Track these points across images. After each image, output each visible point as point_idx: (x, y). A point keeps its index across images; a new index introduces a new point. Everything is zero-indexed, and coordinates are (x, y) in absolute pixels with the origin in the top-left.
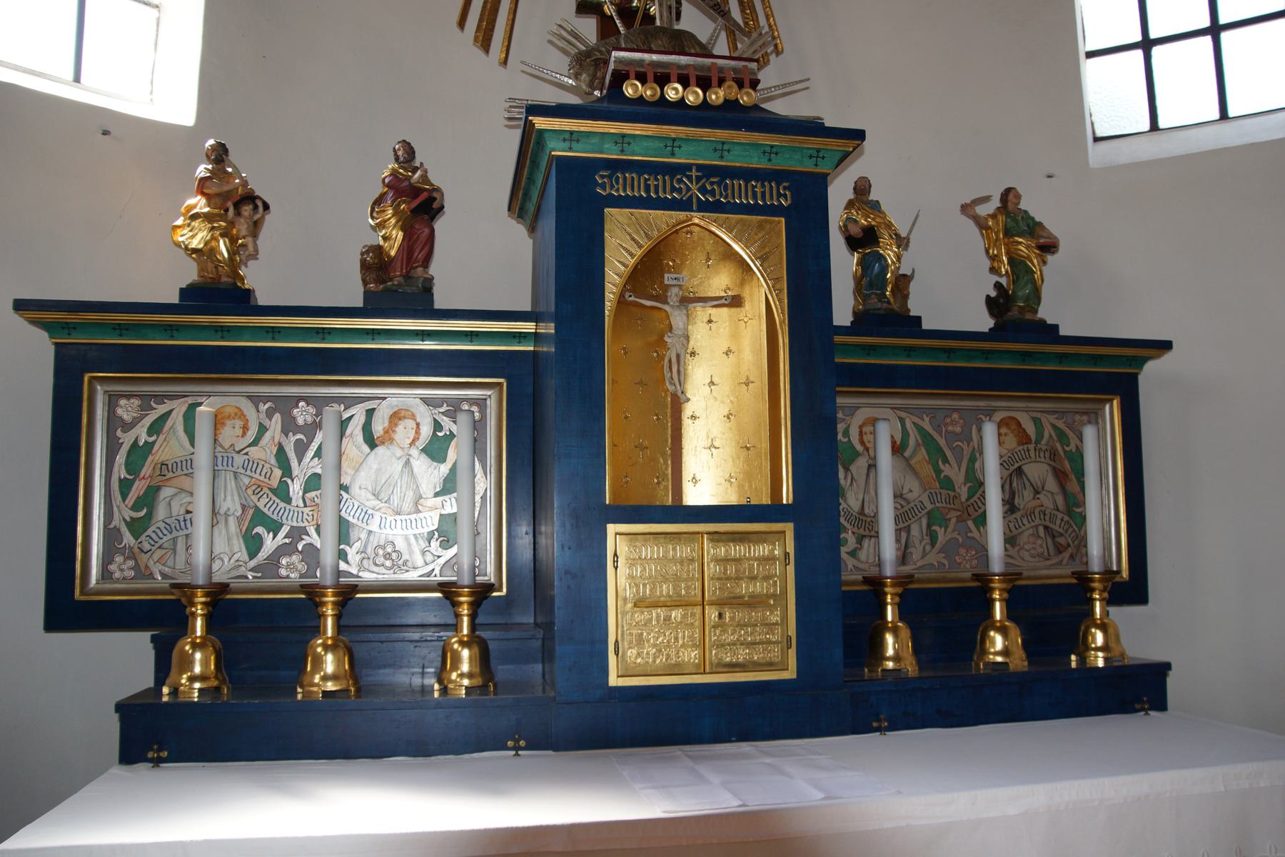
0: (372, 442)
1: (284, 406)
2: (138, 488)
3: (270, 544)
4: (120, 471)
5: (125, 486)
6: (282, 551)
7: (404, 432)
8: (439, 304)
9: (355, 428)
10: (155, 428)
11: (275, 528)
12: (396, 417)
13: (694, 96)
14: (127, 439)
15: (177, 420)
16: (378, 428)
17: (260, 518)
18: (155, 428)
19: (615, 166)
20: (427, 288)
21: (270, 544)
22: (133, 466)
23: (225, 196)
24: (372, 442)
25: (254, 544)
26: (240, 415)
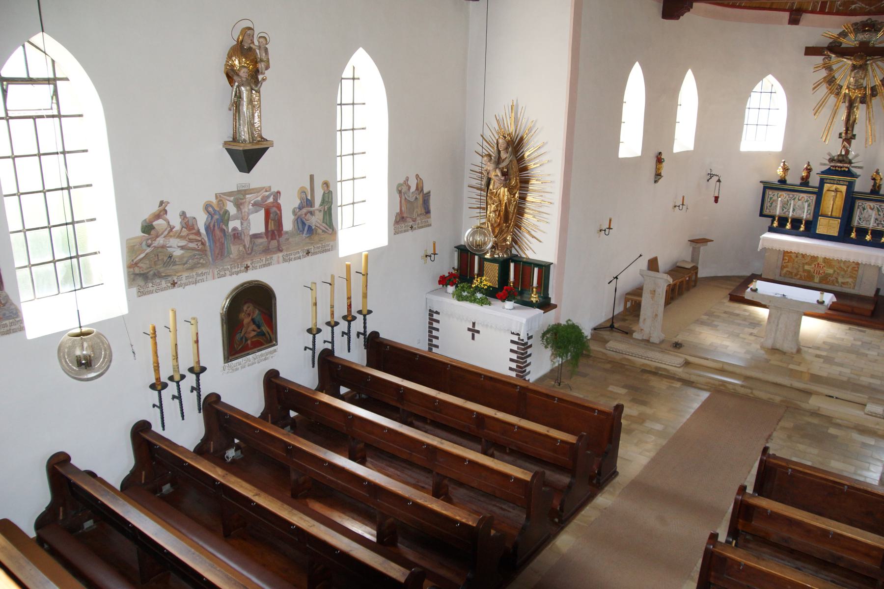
0: (799, 200)
1: (789, 194)
2: (771, 202)
3: (785, 210)
4: (769, 200)
5: (769, 202)
6: (787, 211)
7: (803, 199)
8: (810, 184)
9: (797, 198)
10: (773, 195)
11: (786, 208)
12: (802, 197)
13: (839, 169)
14: (770, 196)
15: (776, 195)
16: (800, 198)
17: (784, 207)
18: (773, 195)
19: (827, 179)
20: (808, 182)
21: (785, 210)
22: (770, 199)
23: (785, 168)
24: (799, 200)
25: (783, 210)
26: (783, 195)
